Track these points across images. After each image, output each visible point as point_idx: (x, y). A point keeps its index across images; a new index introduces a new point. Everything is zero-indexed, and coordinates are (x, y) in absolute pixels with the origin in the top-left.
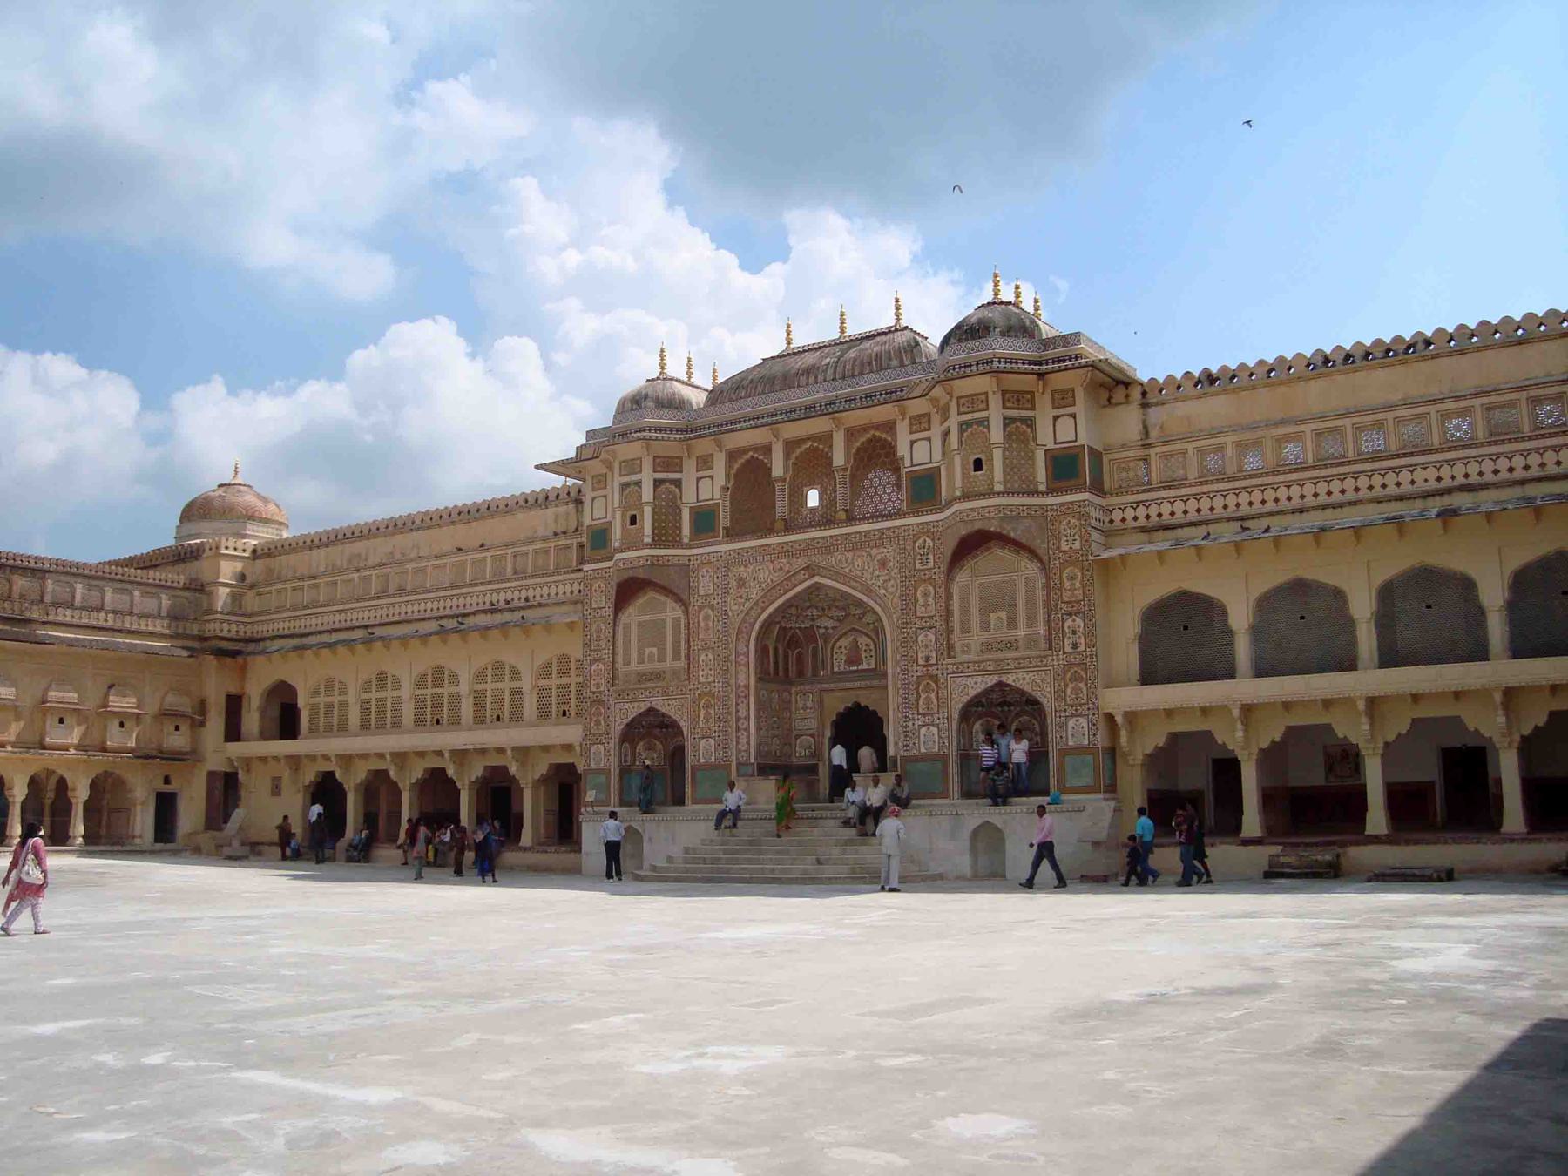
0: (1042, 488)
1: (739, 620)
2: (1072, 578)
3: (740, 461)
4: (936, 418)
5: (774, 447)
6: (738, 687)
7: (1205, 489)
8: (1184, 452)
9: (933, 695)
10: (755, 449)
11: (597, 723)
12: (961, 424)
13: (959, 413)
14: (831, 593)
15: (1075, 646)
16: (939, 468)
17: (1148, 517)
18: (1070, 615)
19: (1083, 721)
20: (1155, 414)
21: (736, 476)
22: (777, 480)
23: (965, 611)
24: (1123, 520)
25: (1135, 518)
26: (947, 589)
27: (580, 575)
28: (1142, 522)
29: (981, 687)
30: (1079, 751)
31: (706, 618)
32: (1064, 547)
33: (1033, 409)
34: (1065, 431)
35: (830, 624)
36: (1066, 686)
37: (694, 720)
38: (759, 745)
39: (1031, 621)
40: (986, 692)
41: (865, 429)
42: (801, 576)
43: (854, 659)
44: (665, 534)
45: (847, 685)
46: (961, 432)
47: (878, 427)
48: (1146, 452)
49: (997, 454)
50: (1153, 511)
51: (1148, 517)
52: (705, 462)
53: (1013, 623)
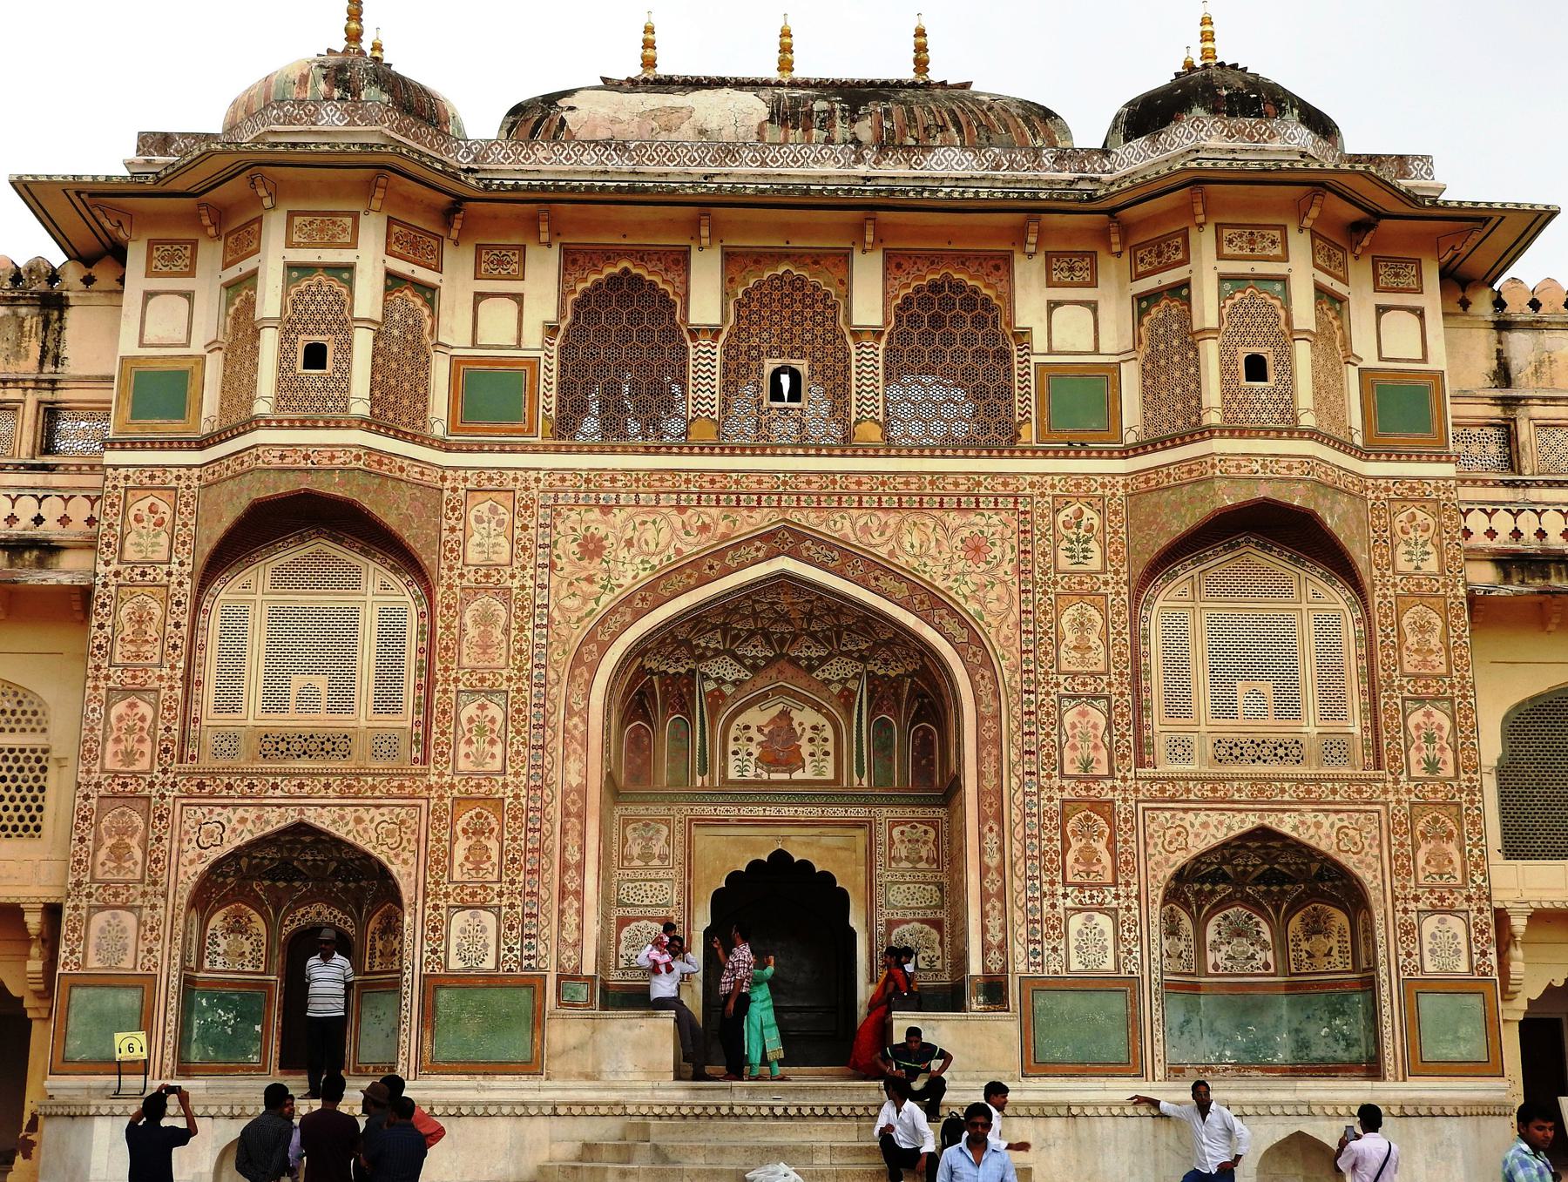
0: (1358, 440)
1: (579, 633)
2: (1423, 628)
3: (593, 277)
4: (1112, 270)
5: (696, 258)
9: (1101, 846)
10: (641, 255)
11: (119, 853)
12: (1223, 278)
13: (1221, 256)
15: (1432, 766)
17: (1517, 534)
18: (1421, 700)
19: (1456, 925)
20: (1521, 346)
22: (694, 333)
23: (1177, 666)
24: (1467, 533)
25: (1491, 533)
26: (1134, 620)
27: (95, 481)
28: (1503, 542)
29: (1221, 836)
30: (1450, 986)
31: (486, 619)
32: (1402, 564)
36: (1416, 847)
37: (439, 862)
39: (1332, 706)
44: (395, 408)
45: (758, 811)
46: (1222, 297)
50: (1528, 524)
51: (1517, 534)
52: (498, 260)
53: (1289, 706)
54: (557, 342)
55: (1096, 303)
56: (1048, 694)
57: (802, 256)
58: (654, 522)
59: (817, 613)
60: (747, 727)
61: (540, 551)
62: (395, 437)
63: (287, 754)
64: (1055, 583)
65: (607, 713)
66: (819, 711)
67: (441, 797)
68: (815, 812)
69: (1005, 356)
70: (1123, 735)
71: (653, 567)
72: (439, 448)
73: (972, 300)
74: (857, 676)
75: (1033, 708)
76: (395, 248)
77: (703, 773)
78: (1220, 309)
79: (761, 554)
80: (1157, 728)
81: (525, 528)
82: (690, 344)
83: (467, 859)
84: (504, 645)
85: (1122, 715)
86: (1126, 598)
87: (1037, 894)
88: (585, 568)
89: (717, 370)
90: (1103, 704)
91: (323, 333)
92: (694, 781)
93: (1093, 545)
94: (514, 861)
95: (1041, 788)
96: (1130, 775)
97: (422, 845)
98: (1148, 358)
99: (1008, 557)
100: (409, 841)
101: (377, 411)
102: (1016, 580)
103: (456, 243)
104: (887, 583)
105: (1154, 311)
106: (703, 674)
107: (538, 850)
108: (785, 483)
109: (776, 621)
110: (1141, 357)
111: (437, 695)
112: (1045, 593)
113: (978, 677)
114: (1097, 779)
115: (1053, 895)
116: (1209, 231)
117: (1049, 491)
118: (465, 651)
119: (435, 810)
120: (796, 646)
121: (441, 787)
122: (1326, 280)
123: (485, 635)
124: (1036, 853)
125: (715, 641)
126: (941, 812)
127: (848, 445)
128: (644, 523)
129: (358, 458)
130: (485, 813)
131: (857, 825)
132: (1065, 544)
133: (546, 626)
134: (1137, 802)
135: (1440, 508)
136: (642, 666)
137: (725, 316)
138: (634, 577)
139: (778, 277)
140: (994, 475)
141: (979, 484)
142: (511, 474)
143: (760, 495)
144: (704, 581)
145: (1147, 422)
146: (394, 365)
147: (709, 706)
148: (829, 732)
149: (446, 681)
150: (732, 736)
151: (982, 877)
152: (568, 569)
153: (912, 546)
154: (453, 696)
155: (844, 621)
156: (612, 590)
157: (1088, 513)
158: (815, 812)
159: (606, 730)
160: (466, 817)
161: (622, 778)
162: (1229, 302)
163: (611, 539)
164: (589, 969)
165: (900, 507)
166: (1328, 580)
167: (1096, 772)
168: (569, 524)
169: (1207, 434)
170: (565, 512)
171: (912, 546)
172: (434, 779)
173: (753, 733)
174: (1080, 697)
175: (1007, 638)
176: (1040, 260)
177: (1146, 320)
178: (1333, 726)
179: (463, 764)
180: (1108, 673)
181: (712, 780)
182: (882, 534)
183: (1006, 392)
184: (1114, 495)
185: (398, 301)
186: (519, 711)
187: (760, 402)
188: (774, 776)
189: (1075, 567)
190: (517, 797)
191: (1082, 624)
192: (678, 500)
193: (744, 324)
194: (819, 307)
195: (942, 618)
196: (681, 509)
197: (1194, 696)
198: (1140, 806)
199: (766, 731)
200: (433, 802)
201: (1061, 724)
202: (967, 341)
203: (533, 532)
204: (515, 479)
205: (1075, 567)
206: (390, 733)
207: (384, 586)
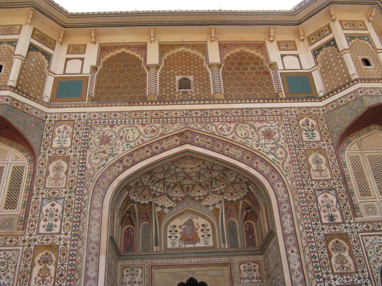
1: (99, 173)
3: (111, 54)
6: (90, 241)
9: (346, 254)
12: (346, 35)
13: (343, 29)
14: (189, 166)
16: (310, 73)
21: (105, 63)
22: (148, 67)
23: (360, 174)
31: (58, 168)
35: (167, 203)
41: (237, 44)
42: (172, 141)
43: (190, 236)
45: (181, 261)
46: (348, 41)
47: (247, 45)
54: (96, 74)
55: (298, 55)
56: (309, 189)
57: (188, 45)
58: (132, 130)
59: (202, 172)
60: (175, 226)
61: (83, 142)
62: (26, 97)
64: (303, 146)
65: (112, 210)
66: (205, 218)
67: (29, 246)
68: (206, 260)
69: (267, 73)
70: (345, 204)
71: (131, 147)
72: (46, 106)
73: (252, 57)
74: (220, 202)
75: (303, 195)
76: (35, 37)
77: (157, 245)
78: (348, 44)
79: (178, 143)
80: (359, 201)
81: (78, 133)
82: (147, 72)
83: (39, 275)
84: (65, 179)
85: (343, 196)
86: (333, 150)
87: (321, 280)
88: (102, 148)
89: (158, 80)
90: (333, 192)
91: (2, 61)
92: (153, 249)
93: (315, 132)
94: (61, 275)
95: (314, 230)
96: (352, 221)
97: (18, 268)
98: (322, 68)
99: (282, 137)
100: (11, 267)
101: (19, 88)
102: (287, 145)
103: (61, 44)
104: (233, 151)
105: (321, 53)
106: (155, 204)
107: (74, 270)
108: (186, 114)
109: (185, 178)
110: (319, 69)
111: (33, 200)
112: (300, 149)
113: (276, 186)
114: (338, 224)
115: (329, 279)
117: (294, 113)
118: (48, 182)
119: (25, 252)
120: (194, 191)
121: (30, 241)
124: (317, 259)
126: (260, 257)
127: (211, 100)
128: (129, 130)
129: (7, 100)
130: (50, 252)
131: (224, 264)
132: (304, 132)
133: (84, 171)
134: (358, 233)
136: (128, 197)
137: (160, 62)
138: (123, 150)
139: (179, 52)
140: (271, 109)
141: (266, 112)
142: (74, 115)
143: (176, 118)
144: (154, 154)
145: (327, 88)
146: (30, 75)
147: (159, 218)
148: (209, 227)
149: (38, 194)
150: (168, 230)
151: (291, 275)
152: (95, 148)
153: (242, 135)
154: (40, 200)
155: (215, 174)
156: (113, 156)
157: (311, 121)
158: (206, 260)
159: (112, 218)
160: (40, 255)
162: (350, 43)
163: (114, 136)
165: (235, 121)
167: (336, 221)
168: (96, 132)
169: (355, 82)
170: (95, 127)
171: (242, 135)
172: (28, 237)
173: (177, 228)
174: (323, 190)
175: (287, 168)
176: (275, 43)
177: (318, 56)
179: (42, 230)
180: (333, 179)
181: (160, 248)
182: (229, 131)
183: (271, 84)
184: (319, 114)
185: (35, 56)
186: (69, 206)
187: (175, 90)
188: (187, 246)
189: (309, 140)
190: (65, 244)
191: (317, 161)
192: (142, 122)
193: (168, 66)
194: (196, 60)
195: (257, 163)
196: (143, 125)
197: (370, 187)
198: (360, 234)
199: (183, 227)
200: (25, 248)
201: (317, 202)
202: (253, 69)
203: (81, 135)
204: (75, 116)
205: (309, 140)
206: (10, 217)
207: (17, 158)
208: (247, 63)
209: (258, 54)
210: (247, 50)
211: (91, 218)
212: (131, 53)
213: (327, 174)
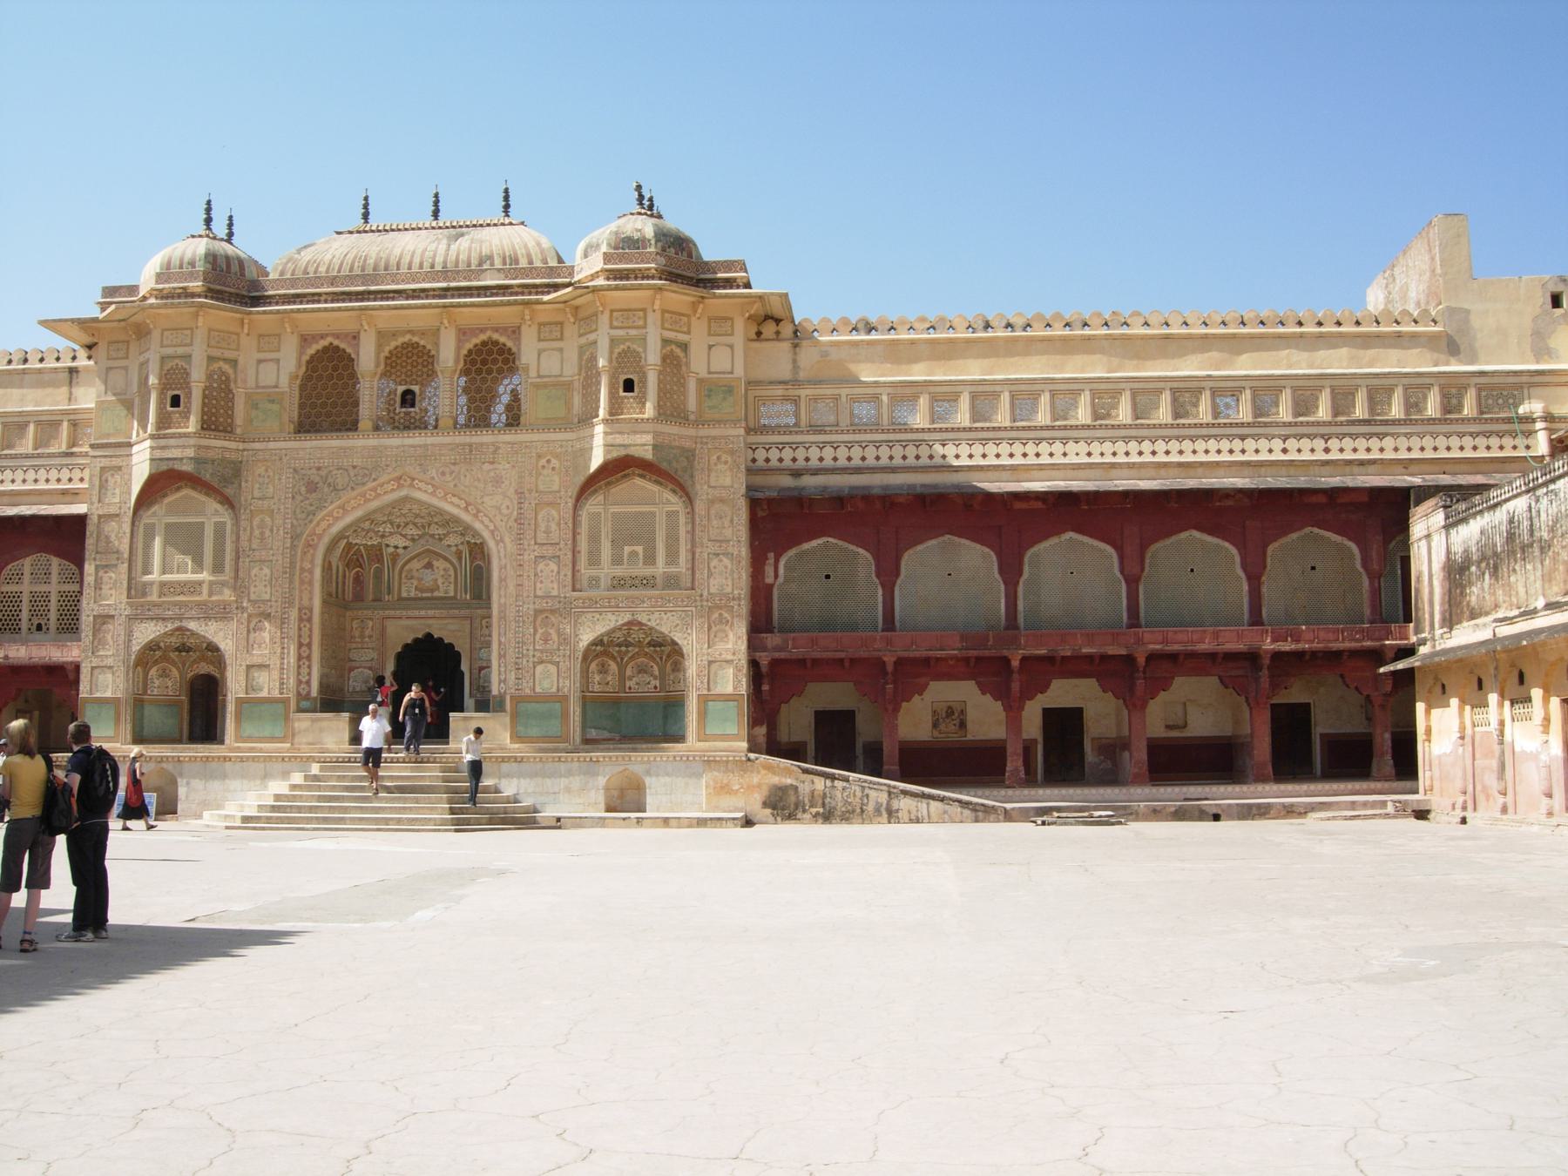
4: (571, 330)
7: (858, 437)
8: (837, 398)
10: (337, 336)
13: (612, 327)
23: (594, 539)
24: (767, 460)
28: (787, 463)
33: (689, 333)
34: (721, 360)
38: (323, 677)
39: (672, 557)
40: (613, 631)
45: (416, 613)
48: (797, 392)
49: (652, 379)
50: (801, 454)
52: (268, 340)
53: (650, 559)
63: (174, 594)
68: (444, 612)
104: (455, 500)
116: (606, 316)
122: (671, 335)
123: (262, 534)
125: (388, 528)
135: (732, 452)
137: (377, 365)
148: (452, 572)
157: (554, 461)
161: (349, 596)
164: (314, 693)
166: (674, 491)
173: (415, 574)
176: (535, 328)
178: (673, 569)
179: (253, 597)
208: (495, 361)
209: (509, 344)
210: (496, 336)
211: (302, 582)
212: (342, 346)
213: (555, 537)
